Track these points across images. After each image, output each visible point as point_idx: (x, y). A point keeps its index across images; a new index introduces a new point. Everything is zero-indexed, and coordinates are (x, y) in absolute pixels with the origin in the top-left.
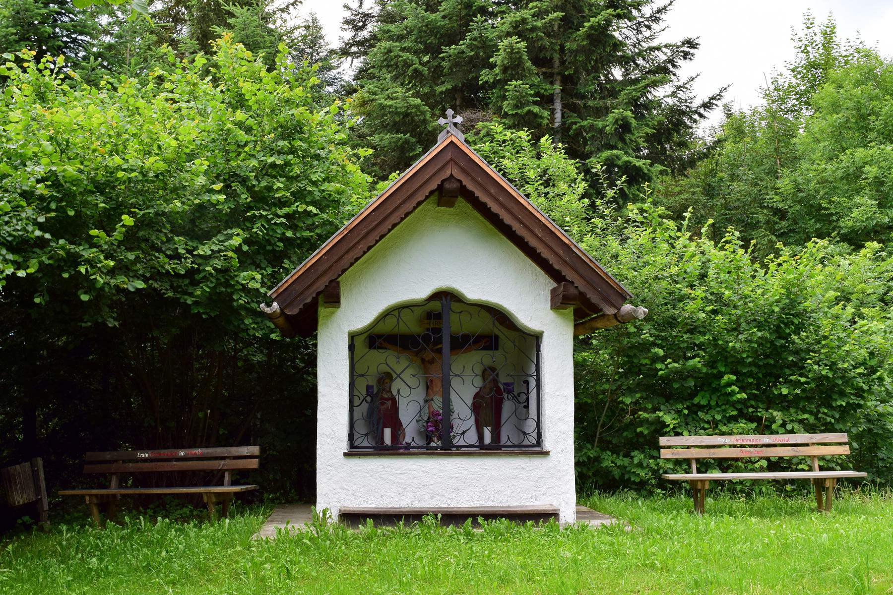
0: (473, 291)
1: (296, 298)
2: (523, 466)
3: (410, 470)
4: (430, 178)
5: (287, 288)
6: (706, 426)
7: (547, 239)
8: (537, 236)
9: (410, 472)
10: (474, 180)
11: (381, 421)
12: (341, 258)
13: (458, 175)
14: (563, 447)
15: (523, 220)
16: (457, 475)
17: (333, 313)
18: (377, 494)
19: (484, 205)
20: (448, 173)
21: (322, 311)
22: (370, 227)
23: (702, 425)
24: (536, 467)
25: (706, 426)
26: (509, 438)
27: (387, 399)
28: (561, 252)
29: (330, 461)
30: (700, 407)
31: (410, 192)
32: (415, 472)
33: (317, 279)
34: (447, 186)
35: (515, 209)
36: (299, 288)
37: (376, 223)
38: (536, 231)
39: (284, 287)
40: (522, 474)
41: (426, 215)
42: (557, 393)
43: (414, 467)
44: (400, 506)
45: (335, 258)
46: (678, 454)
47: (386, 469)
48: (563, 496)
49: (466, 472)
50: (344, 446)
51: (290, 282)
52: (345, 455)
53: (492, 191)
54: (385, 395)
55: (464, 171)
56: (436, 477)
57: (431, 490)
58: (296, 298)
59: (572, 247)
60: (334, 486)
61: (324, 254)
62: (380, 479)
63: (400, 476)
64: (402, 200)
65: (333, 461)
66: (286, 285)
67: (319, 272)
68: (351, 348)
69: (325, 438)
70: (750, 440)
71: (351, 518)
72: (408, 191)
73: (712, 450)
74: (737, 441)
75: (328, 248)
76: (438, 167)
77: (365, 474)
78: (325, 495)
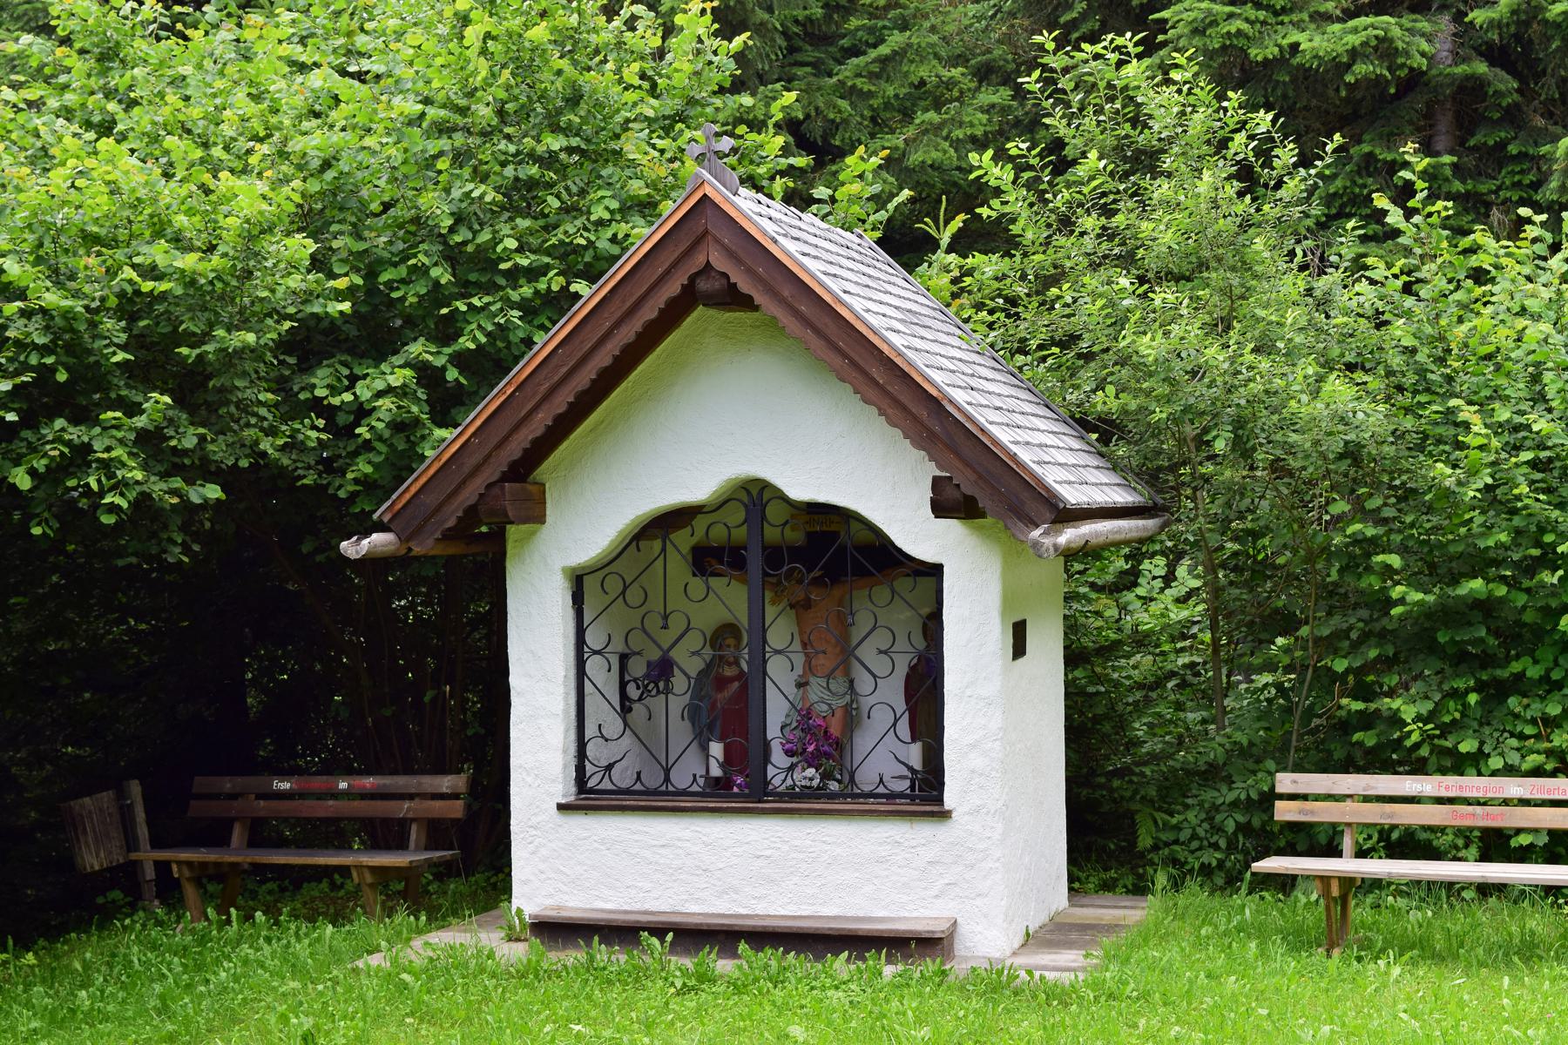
0: (801, 488)
1: (427, 520)
2: (897, 838)
3: (679, 840)
4: (667, 272)
5: (409, 502)
6: (1529, 730)
7: (895, 388)
8: (877, 384)
9: (679, 844)
10: (750, 272)
11: (718, 723)
12: (505, 439)
13: (720, 263)
14: (979, 802)
15: (848, 350)
16: (768, 853)
17: (534, 533)
18: (619, 884)
19: (581, 396)
20: (699, 260)
21: (513, 531)
22: (556, 378)
23: (1519, 729)
24: (923, 841)
25: (1529, 730)
26: (881, 779)
27: (731, 680)
28: (923, 414)
29: (534, 819)
30: (1519, 685)
31: (628, 304)
32: (688, 844)
33: (464, 482)
34: (703, 285)
35: (831, 329)
36: (431, 500)
37: (564, 370)
38: (874, 372)
39: (404, 501)
40: (896, 854)
41: (705, 330)
42: (968, 692)
43: (687, 834)
44: (662, 909)
45: (495, 441)
46: (1312, 812)
47: (636, 837)
48: (978, 902)
49: (785, 848)
50: (563, 789)
51: (413, 490)
52: (562, 807)
53: (786, 293)
54: (729, 672)
55: (731, 255)
56: (728, 854)
57: (720, 880)
58: (427, 520)
59: (945, 403)
60: (542, 866)
61: (474, 434)
62: (624, 855)
63: (662, 851)
64: (613, 320)
65: (540, 819)
66: (408, 496)
67: (466, 470)
68: (578, 599)
69: (524, 774)
70: (1478, 789)
71: (555, 931)
72: (624, 302)
73: (1389, 807)
74: (1447, 788)
75: (478, 423)
76: (682, 248)
77: (596, 845)
78: (525, 882)
